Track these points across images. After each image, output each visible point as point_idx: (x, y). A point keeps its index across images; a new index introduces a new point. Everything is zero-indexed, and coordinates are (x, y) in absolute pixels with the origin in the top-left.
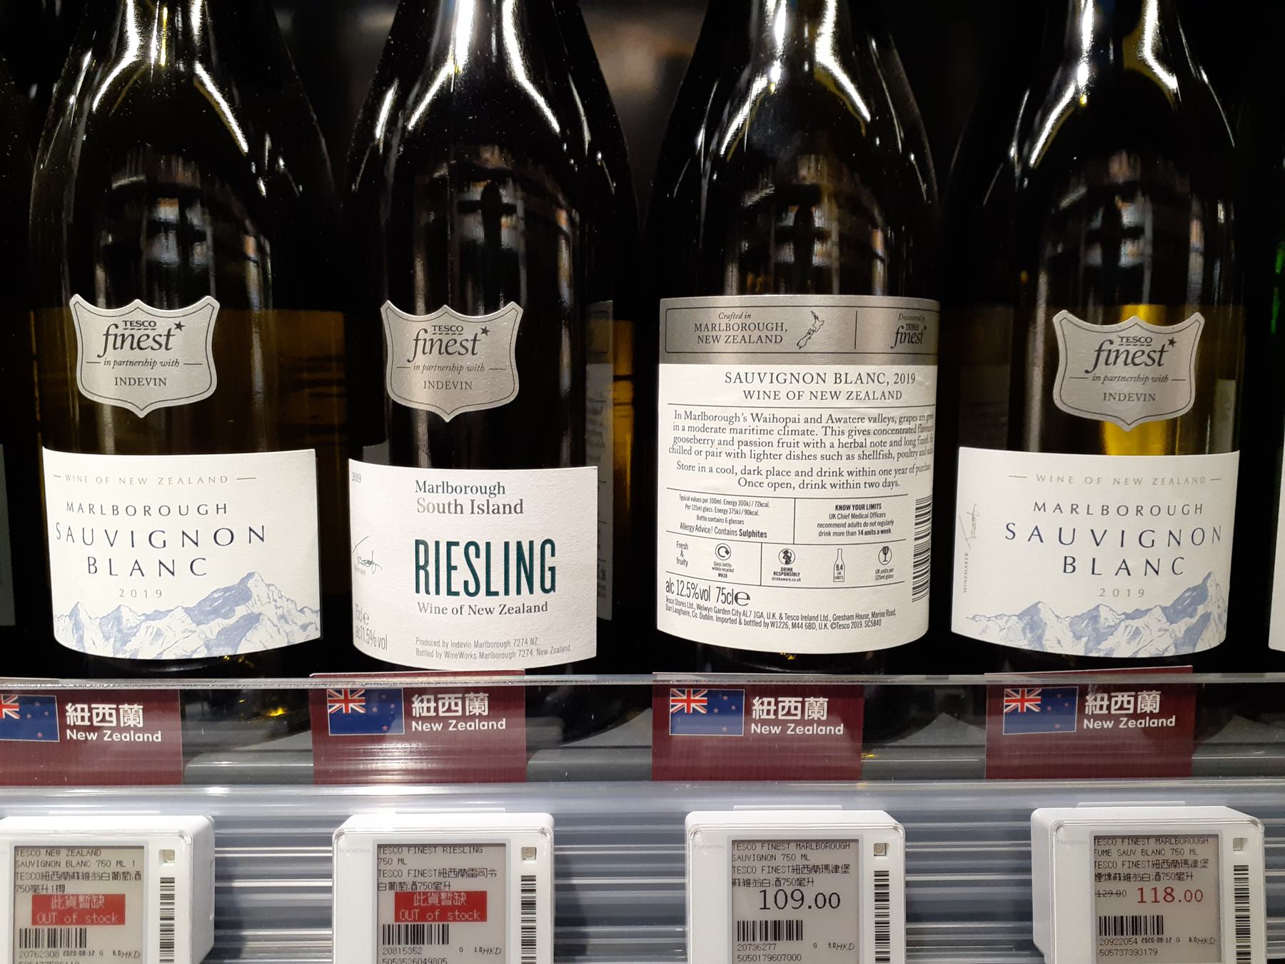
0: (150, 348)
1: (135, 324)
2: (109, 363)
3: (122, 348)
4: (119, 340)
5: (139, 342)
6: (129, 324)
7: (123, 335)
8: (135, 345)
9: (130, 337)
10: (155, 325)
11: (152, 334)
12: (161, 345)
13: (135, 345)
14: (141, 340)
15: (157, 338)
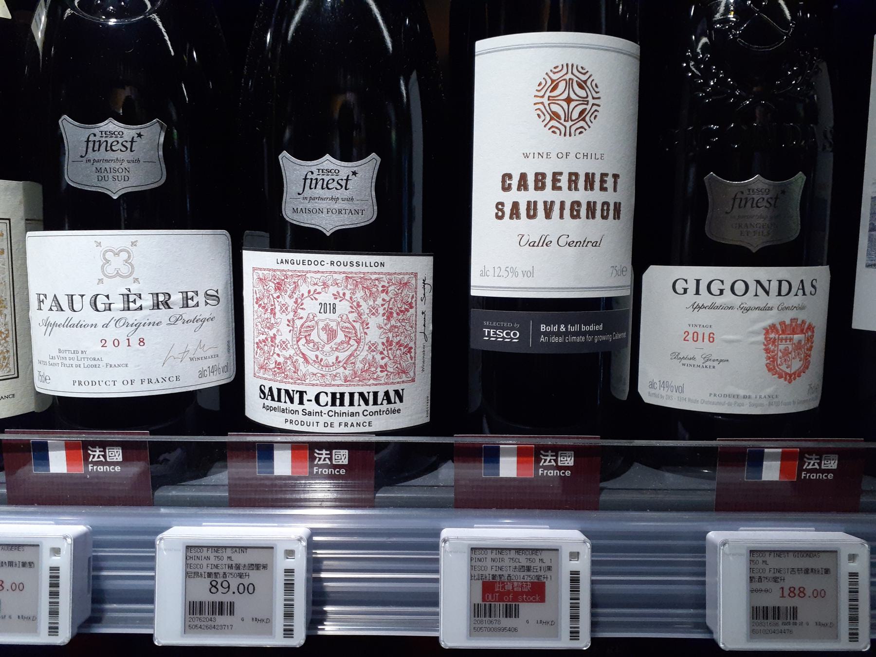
0: (119, 150)
1: (109, 134)
2: (89, 161)
3: (99, 150)
4: (97, 144)
5: (111, 146)
6: (103, 133)
7: (100, 141)
8: (109, 148)
9: (105, 143)
10: (123, 134)
11: (120, 140)
12: (127, 148)
13: (109, 148)
14: (113, 144)
15: (124, 143)
